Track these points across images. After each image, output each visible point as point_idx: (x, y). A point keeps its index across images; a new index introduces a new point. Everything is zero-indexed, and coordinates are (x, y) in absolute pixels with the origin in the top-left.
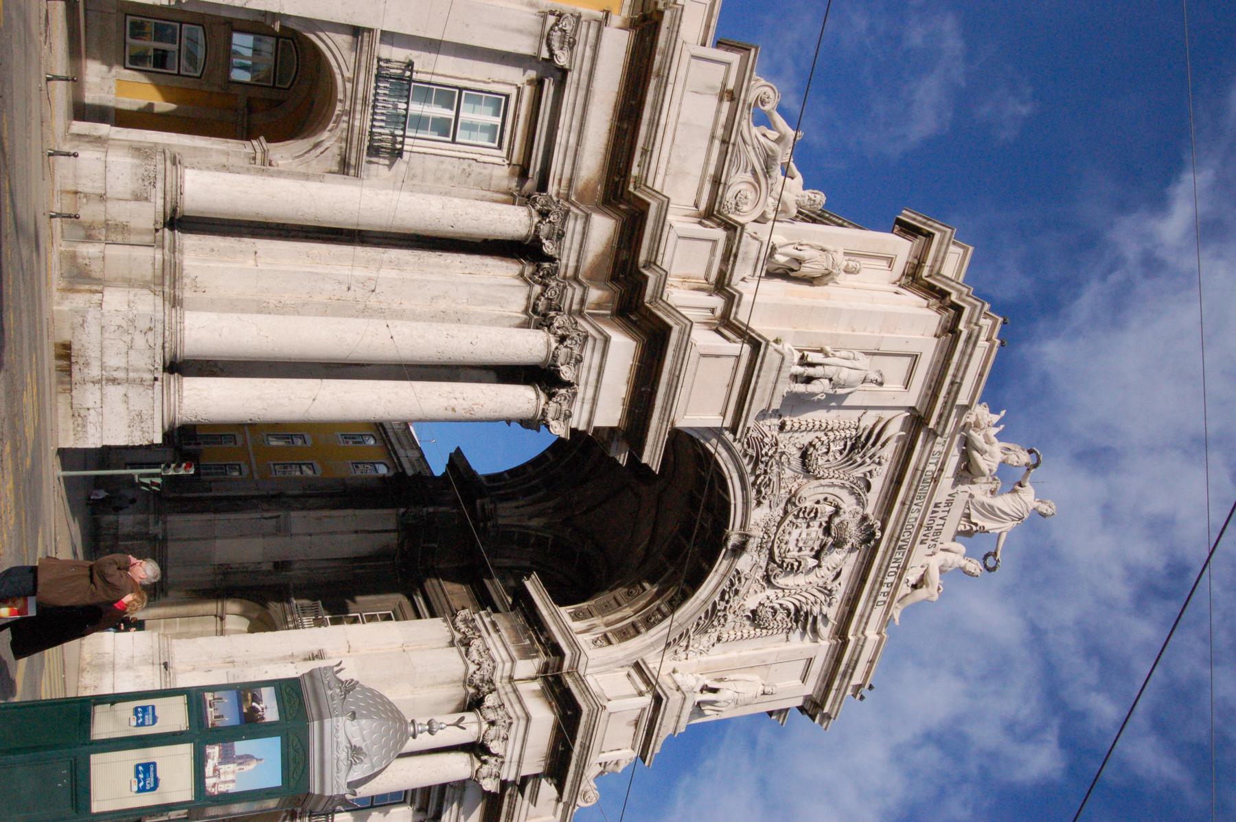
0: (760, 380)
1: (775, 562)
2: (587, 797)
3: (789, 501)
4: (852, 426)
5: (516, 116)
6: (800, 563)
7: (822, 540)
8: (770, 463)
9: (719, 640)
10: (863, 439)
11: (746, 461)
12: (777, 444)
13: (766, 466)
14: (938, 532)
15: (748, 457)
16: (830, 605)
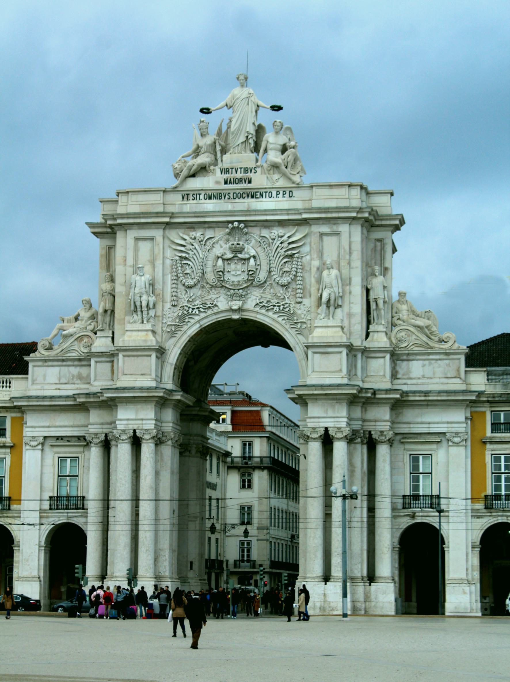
0: (131, 345)
1: (252, 283)
2: (446, 341)
3: (216, 287)
4: (175, 263)
5: (65, 453)
6: (250, 271)
7: (238, 260)
8: (193, 307)
9: (300, 303)
10: (180, 255)
11: (192, 321)
12: (183, 306)
13: (194, 309)
14: (246, 170)
15: (190, 320)
16: (282, 237)
